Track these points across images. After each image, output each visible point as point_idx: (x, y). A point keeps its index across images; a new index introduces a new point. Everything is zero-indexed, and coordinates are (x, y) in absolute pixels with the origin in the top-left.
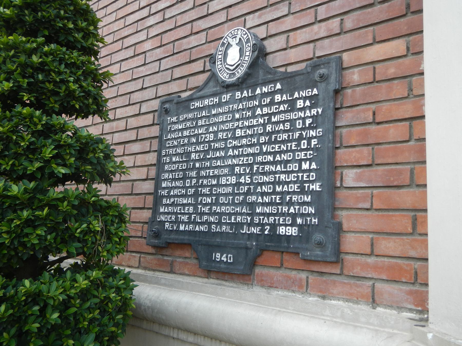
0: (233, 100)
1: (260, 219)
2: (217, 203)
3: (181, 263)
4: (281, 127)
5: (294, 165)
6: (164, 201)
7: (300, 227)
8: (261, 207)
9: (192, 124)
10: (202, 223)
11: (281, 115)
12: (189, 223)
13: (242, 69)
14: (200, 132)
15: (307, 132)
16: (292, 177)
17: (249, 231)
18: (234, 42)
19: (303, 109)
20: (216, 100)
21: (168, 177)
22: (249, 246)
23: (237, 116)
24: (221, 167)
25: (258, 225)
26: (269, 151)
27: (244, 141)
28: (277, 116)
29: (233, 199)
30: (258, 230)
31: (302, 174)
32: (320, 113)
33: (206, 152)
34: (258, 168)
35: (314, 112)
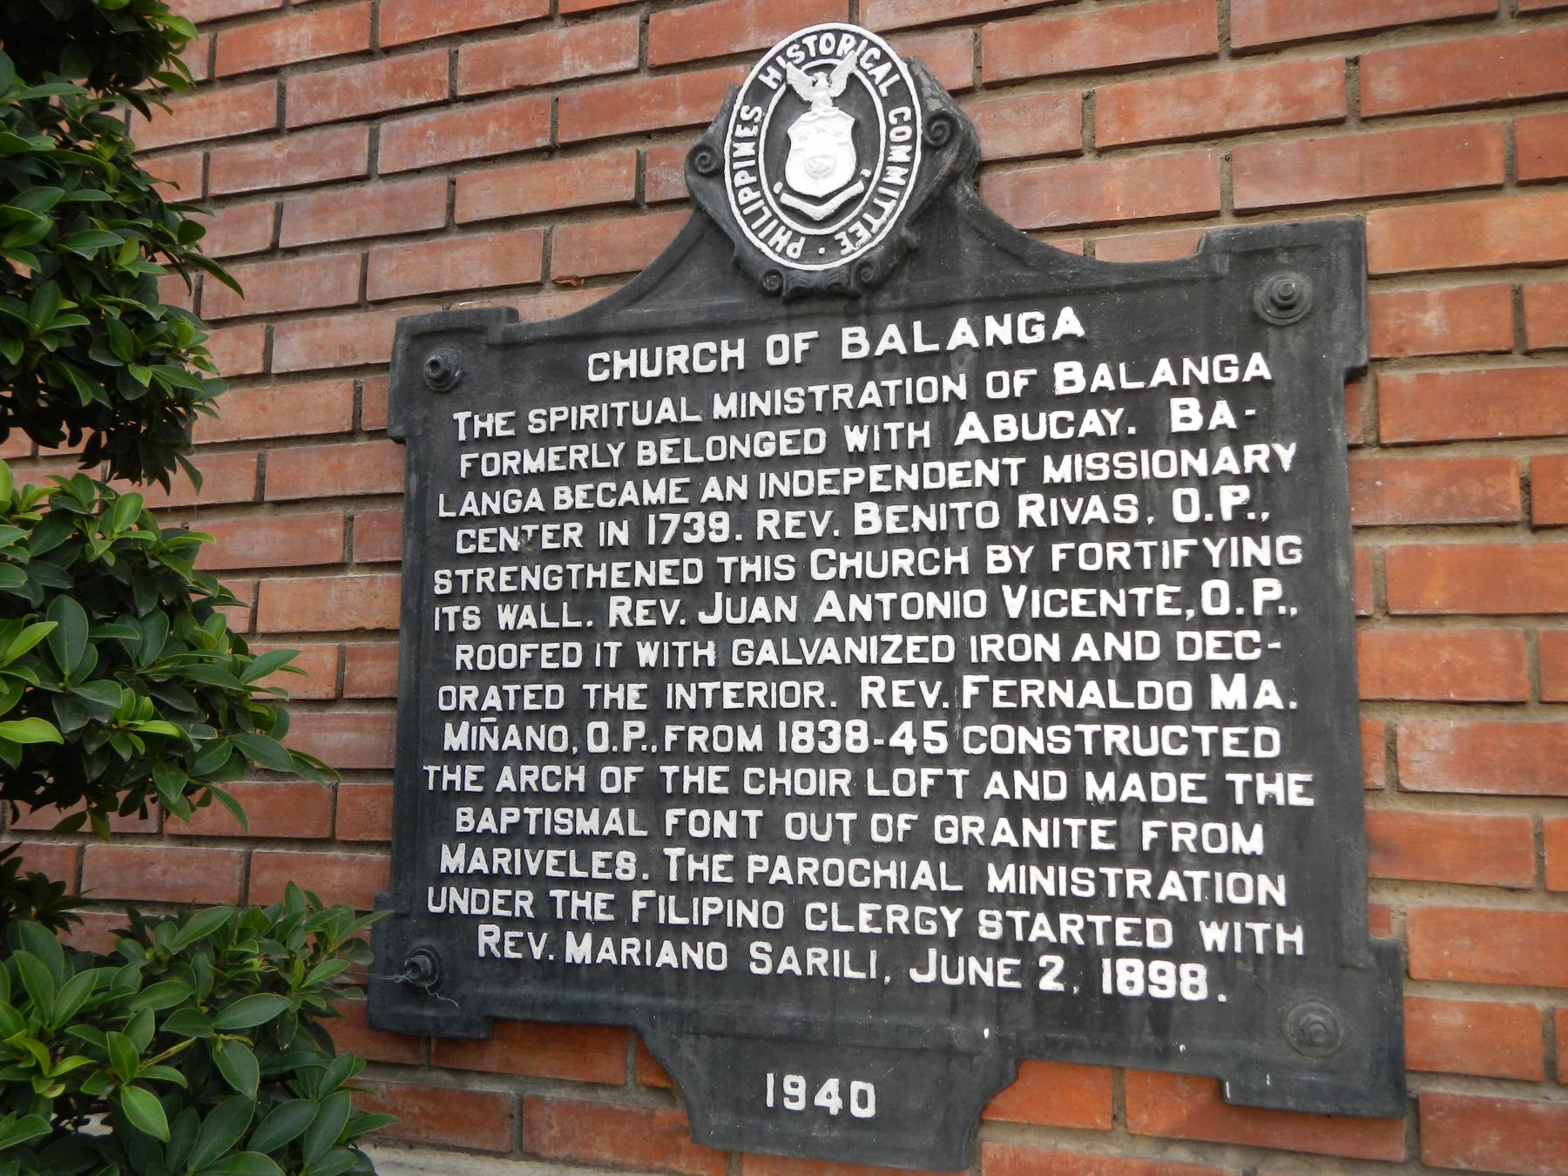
0: (824, 363)
1: (1009, 924)
2: (771, 840)
3: (566, 1109)
4: (1096, 509)
5: (1171, 685)
6: (464, 818)
7: (1220, 964)
8: (1011, 868)
9: (604, 455)
10: (694, 934)
11: (1090, 457)
12: (619, 926)
13: (876, 223)
14: (650, 496)
15: (1228, 546)
16: (1163, 741)
17: (953, 973)
18: (821, 91)
19: (1198, 440)
20: (734, 352)
21: (480, 701)
22: (962, 1044)
23: (855, 438)
25: (1000, 947)
26: (1036, 614)
27: (902, 561)
28: (1067, 459)
29: (860, 828)
30: (1002, 971)
31: (1215, 729)
32: (1286, 466)
33: (697, 597)
34: (986, 689)
35: (1256, 455)
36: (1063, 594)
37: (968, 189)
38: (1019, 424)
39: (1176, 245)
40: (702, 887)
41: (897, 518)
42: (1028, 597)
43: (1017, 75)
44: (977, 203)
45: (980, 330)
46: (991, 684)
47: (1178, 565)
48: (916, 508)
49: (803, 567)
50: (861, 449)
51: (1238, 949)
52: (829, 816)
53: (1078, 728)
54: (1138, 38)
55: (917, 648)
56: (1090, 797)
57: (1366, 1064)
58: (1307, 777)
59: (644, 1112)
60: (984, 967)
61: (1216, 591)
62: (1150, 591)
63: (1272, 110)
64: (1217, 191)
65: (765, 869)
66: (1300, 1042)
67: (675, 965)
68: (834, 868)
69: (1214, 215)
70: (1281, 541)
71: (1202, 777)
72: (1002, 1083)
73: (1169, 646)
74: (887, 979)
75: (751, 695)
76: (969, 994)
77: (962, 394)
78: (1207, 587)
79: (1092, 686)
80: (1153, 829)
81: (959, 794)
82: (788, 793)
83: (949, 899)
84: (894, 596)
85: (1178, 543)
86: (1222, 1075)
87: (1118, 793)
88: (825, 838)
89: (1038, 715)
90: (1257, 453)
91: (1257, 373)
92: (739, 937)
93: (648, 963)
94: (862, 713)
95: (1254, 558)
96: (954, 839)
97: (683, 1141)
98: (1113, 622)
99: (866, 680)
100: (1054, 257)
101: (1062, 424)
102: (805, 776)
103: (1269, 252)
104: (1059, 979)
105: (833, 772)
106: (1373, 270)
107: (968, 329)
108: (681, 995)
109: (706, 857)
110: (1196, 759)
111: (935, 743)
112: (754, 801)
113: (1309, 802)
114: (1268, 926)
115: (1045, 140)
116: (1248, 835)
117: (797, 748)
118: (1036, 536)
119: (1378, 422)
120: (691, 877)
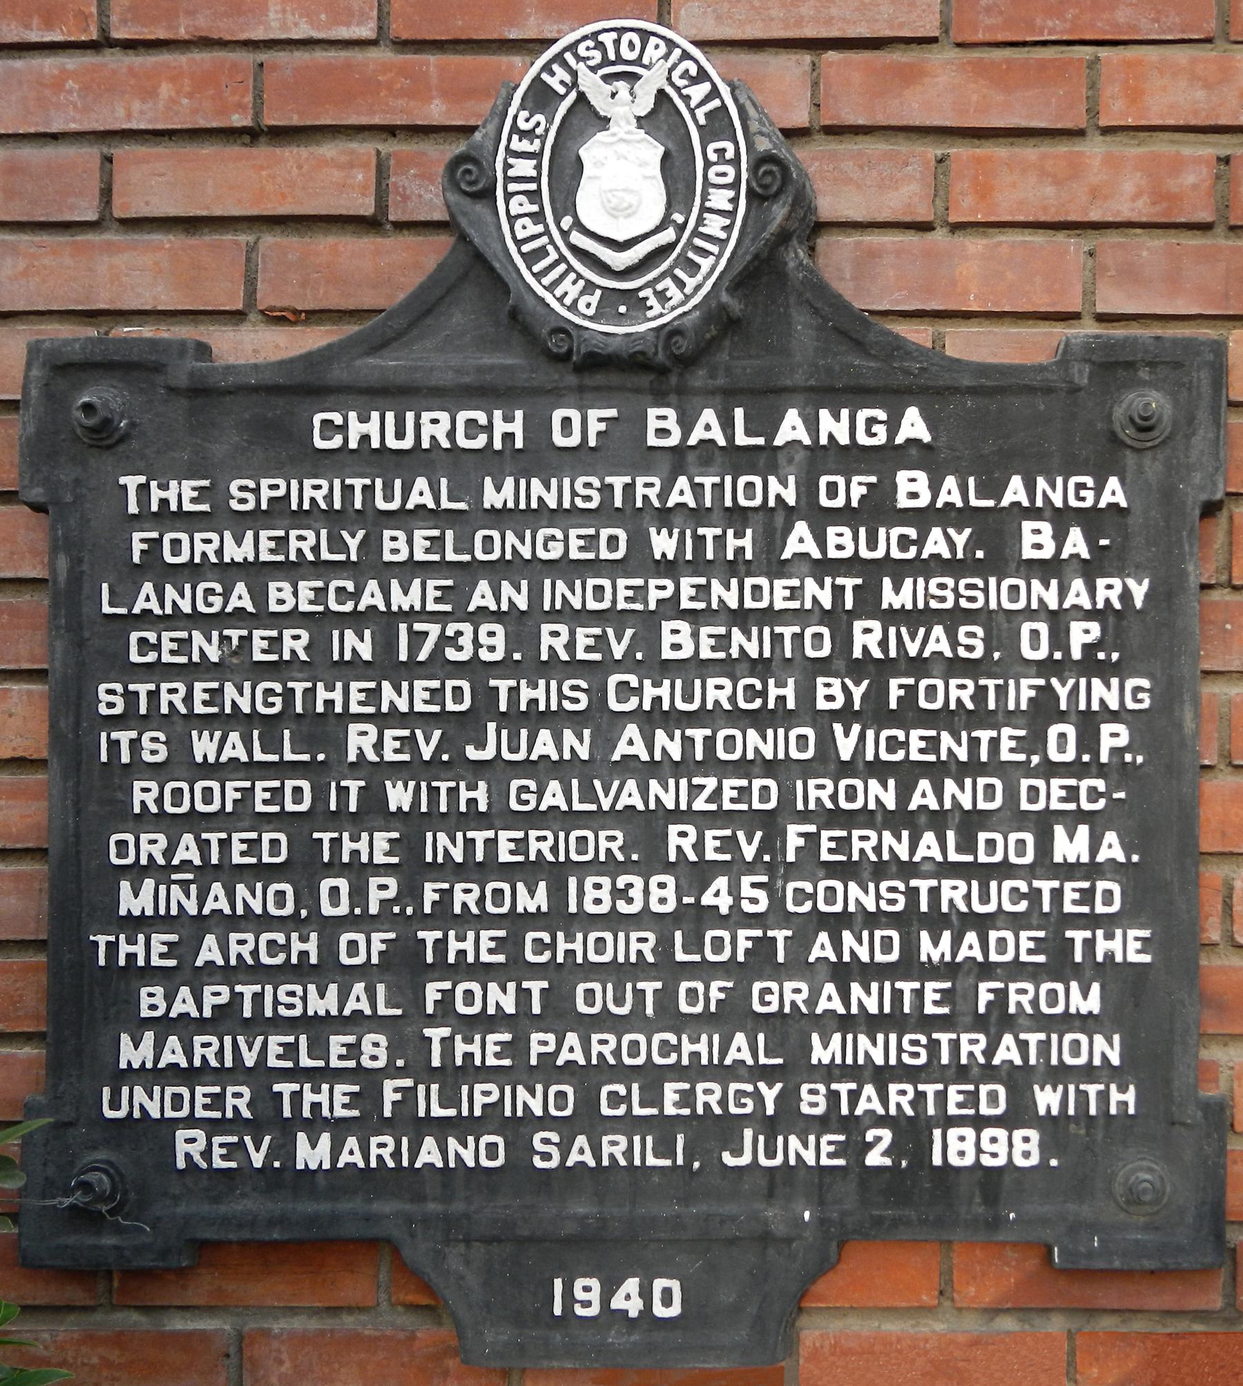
0: (623, 449)
1: (833, 1097)
2: (559, 1014)
4: (939, 642)
5: (1013, 837)
6: (151, 1000)
7: (1053, 1129)
8: (837, 1037)
9: (337, 544)
10: (464, 1127)
11: (934, 582)
13: (691, 283)
14: (399, 600)
15: (1076, 687)
16: (1003, 896)
17: (771, 1154)
18: (624, 107)
19: (1049, 569)
20: (510, 426)
21: (169, 853)
22: (779, 1229)
23: (663, 544)
24: (570, 819)
25: (823, 1124)
26: (870, 757)
27: (718, 691)
28: (908, 582)
29: (666, 998)
30: (826, 1149)
31: (1056, 884)
32: (1139, 604)
33: (466, 727)
34: (812, 840)
35: (1109, 590)
36: (901, 735)
37: (801, 254)
38: (856, 539)
39: (1030, 347)
40: (473, 1072)
41: (712, 642)
42: (862, 737)
43: (861, 122)
44: (812, 272)
45: (812, 425)
46: (818, 834)
47: (1024, 707)
48: (735, 630)
49: (598, 695)
50: (670, 557)
51: (1071, 1112)
52: (629, 986)
53: (914, 883)
54: (1000, 98)
55: (735, 794)
56: (924, 958)
57: (1189, 1219)
58: (1146, 933)
59: (401, 1335)
60: (806, 1146)
61: (1062, 736)
62: (994, 734)
63: (1140, 203)
64: (1079, 289)
65: (551, 1048)
66: (1128, 1202)
67: (440, 1164)
68: (634, 1045)
69: (1073, 317)
70: (1131, 683)
71: (1041, 934)
72: (824, 1266)
73: (1012, 794)
74: (696, 1165)
75: (534, 846)
76: (787, 1178)
77: (791, 501)
78: (1053, 731)
79: (929, 838)
80: (990, 991)
81: (781, 958)
82: (579, 960)
83: (768, 1073)
84: (708, 732)
85: (1024, 682)
86: (1051, 1241)
87: (954, 954)
88: (624, 1010)
89: (870, 869)
90: (1109, 587)
91: (1113, 500)
92: (518, 1129)
93: (405, 1163)
94: (668, 867)
95: (1102, 702)
96: (774, 1008)
97: (452, 1363)
98: (953, 768)
99: (673, 829)
100: (898, 347)
101: (904, 542)
102: (600, 941)
103: (1130, 365)
104: (886, 1153)
105: (634, 936)
106: (1233, 397)
107: (799, 423)
108: (447, 1198)
109: (477, 1038)
110: (1035, 915)
111: (754, 901)
112: (537, 971)
113: (1146, 958)
114: (1102, 1087)
115: (892, 205)
116: (1085, 994)
117: (590, 908)
118: (871, 668)
119: (1230, 561)
120: (459, 1062)
